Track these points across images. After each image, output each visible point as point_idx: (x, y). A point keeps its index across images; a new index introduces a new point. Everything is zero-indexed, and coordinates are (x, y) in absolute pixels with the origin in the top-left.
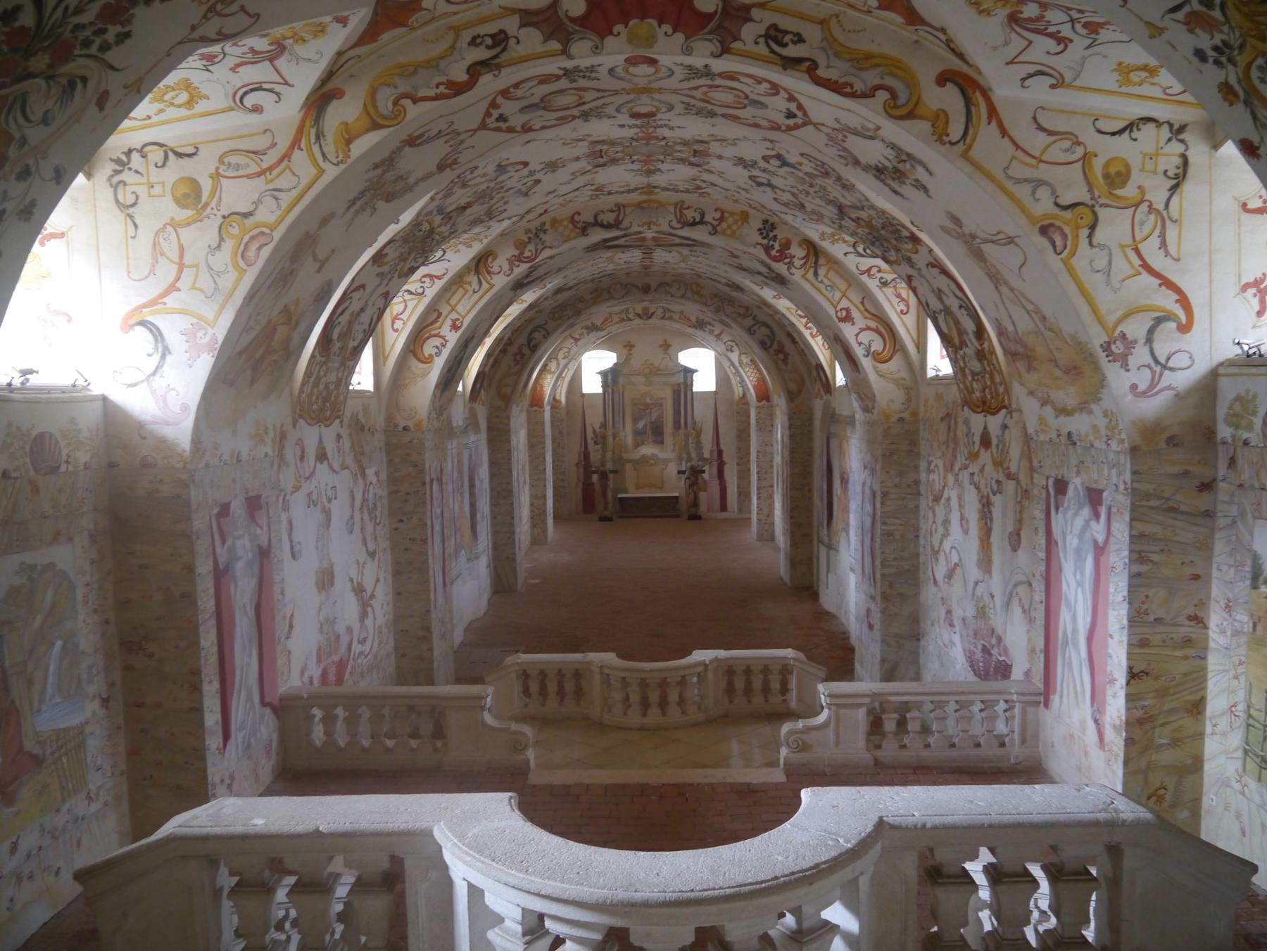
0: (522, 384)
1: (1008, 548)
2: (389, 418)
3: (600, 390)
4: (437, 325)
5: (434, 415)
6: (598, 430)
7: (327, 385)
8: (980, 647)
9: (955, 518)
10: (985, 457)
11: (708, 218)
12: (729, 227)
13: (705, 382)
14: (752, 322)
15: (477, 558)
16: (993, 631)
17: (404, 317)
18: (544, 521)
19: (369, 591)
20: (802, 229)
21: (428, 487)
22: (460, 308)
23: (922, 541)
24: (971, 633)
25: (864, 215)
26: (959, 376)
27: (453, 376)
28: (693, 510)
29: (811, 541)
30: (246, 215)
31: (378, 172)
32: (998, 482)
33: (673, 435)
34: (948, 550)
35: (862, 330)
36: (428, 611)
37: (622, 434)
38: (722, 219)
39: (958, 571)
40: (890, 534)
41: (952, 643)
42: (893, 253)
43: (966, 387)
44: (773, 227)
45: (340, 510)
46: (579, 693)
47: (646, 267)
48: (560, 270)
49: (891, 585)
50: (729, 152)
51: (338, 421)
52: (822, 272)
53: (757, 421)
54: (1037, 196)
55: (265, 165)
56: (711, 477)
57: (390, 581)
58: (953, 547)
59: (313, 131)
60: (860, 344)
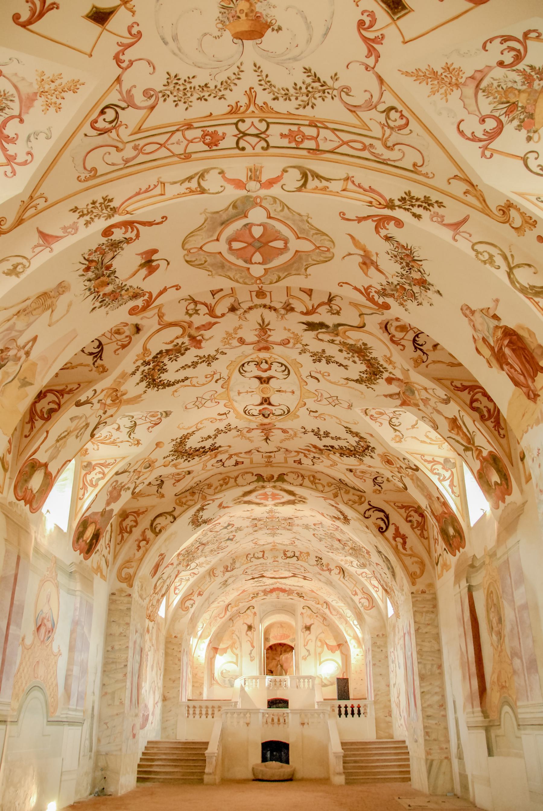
25: (199, 551)
42: (182, 558)
50: (246, 531)
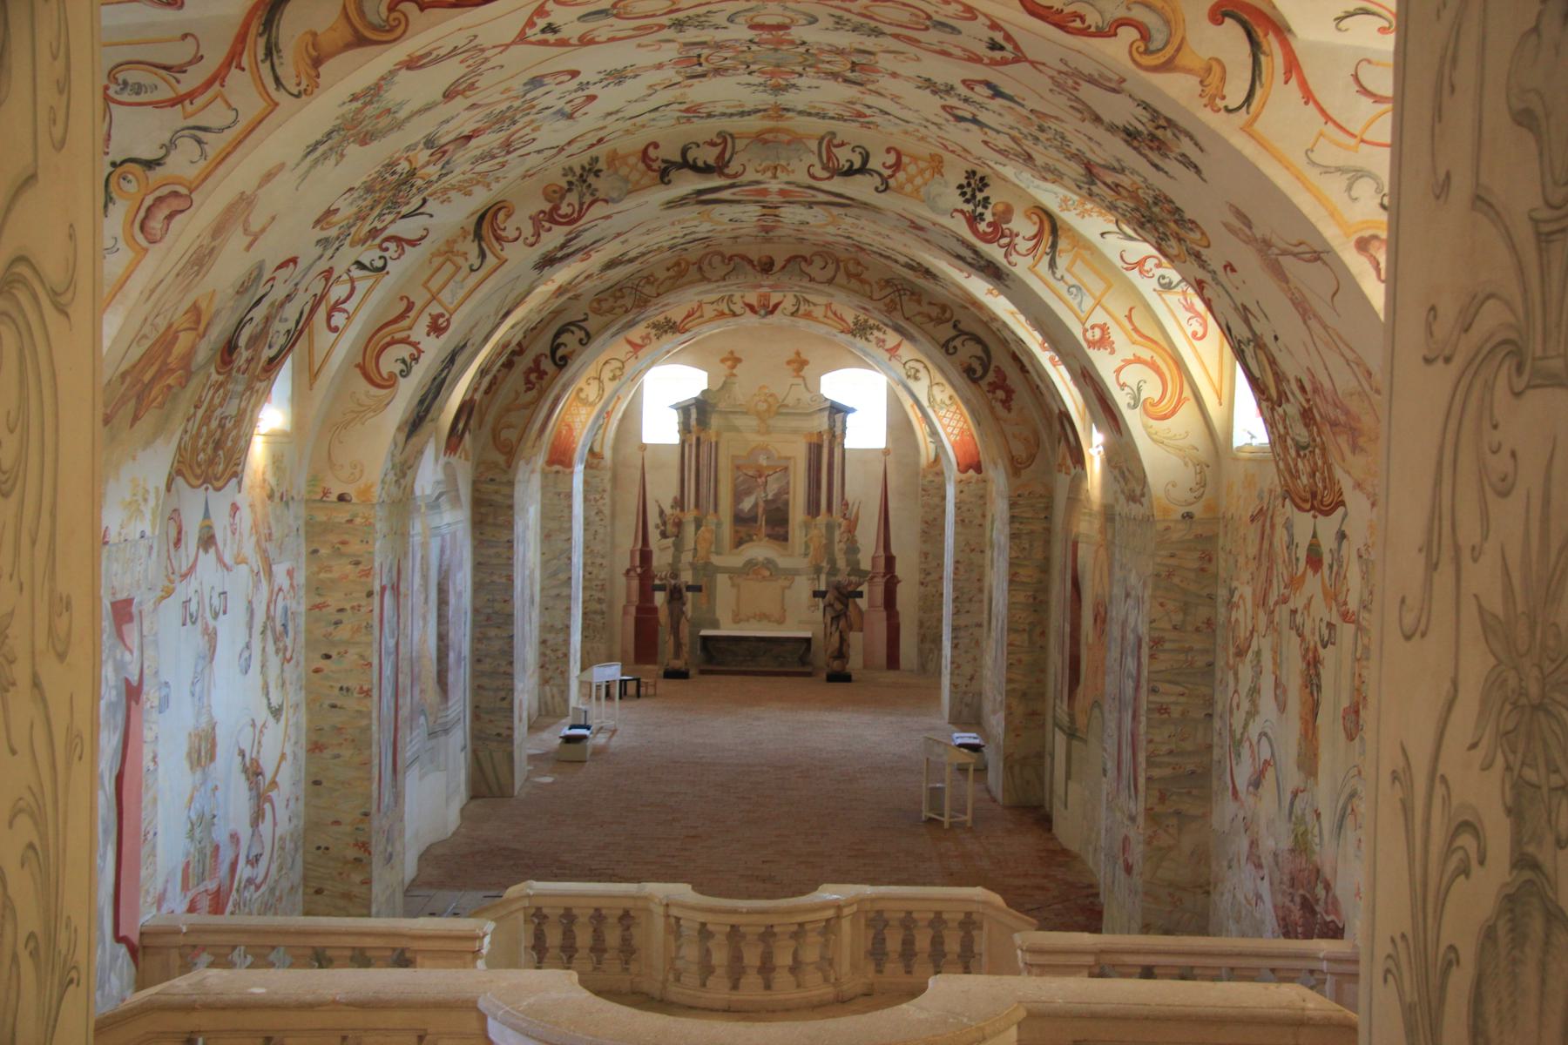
0: (537, 425)
1: (1342, 736)
2: (314, 480)
3: (674, 438)
4: (406, 323)
5: (391, 477)
6: (668, 511)
7: (221, 426)
8: (1298, 900)
9: (1267, 683)
10: (1313, 585)
11: (869, 166)
12: (910, 180)
13: (866, 432)
14: (954, 333)
15: (446, 731)
16: (1318, 871)
17: (349, 306)
18: (564, 674)
19: (269, 775)
20: (1032, 191)
21: (377, 598)
22: (445, 296)
23: (1217, 724)
24: (1286, 878)
25: (1125, 180)
26: (1278, 449)
27: (427, 410)
28: (836, 665)
29: (1043, 726)
30: (150, 164)
31: (358, 104)
32: (1330, 626)
33: (807, 526)
34: (1255, 739)
35: (1128, 362)
36: (366, 814)
37: (711, 518)
38: (897, 166)
39: (1270, 774)
40: (1163, 709)
41: (1259, 897)
42: (1173, 242)
43: (1287, 464)
44: (983, 183)
45: (231, 632)
46: (628, 950)
47: (767, 230)
48: (619, 235)
49: (1162, 798)
51: (234, 481)
52: (1062, 262)
53: (958, 507)
54: (1354, 194)
55: (183, 89)
56: (871, 605)
57: (303, 762)
58: (1263, 734)
59: (262, 42)
60: (1123, 386)
